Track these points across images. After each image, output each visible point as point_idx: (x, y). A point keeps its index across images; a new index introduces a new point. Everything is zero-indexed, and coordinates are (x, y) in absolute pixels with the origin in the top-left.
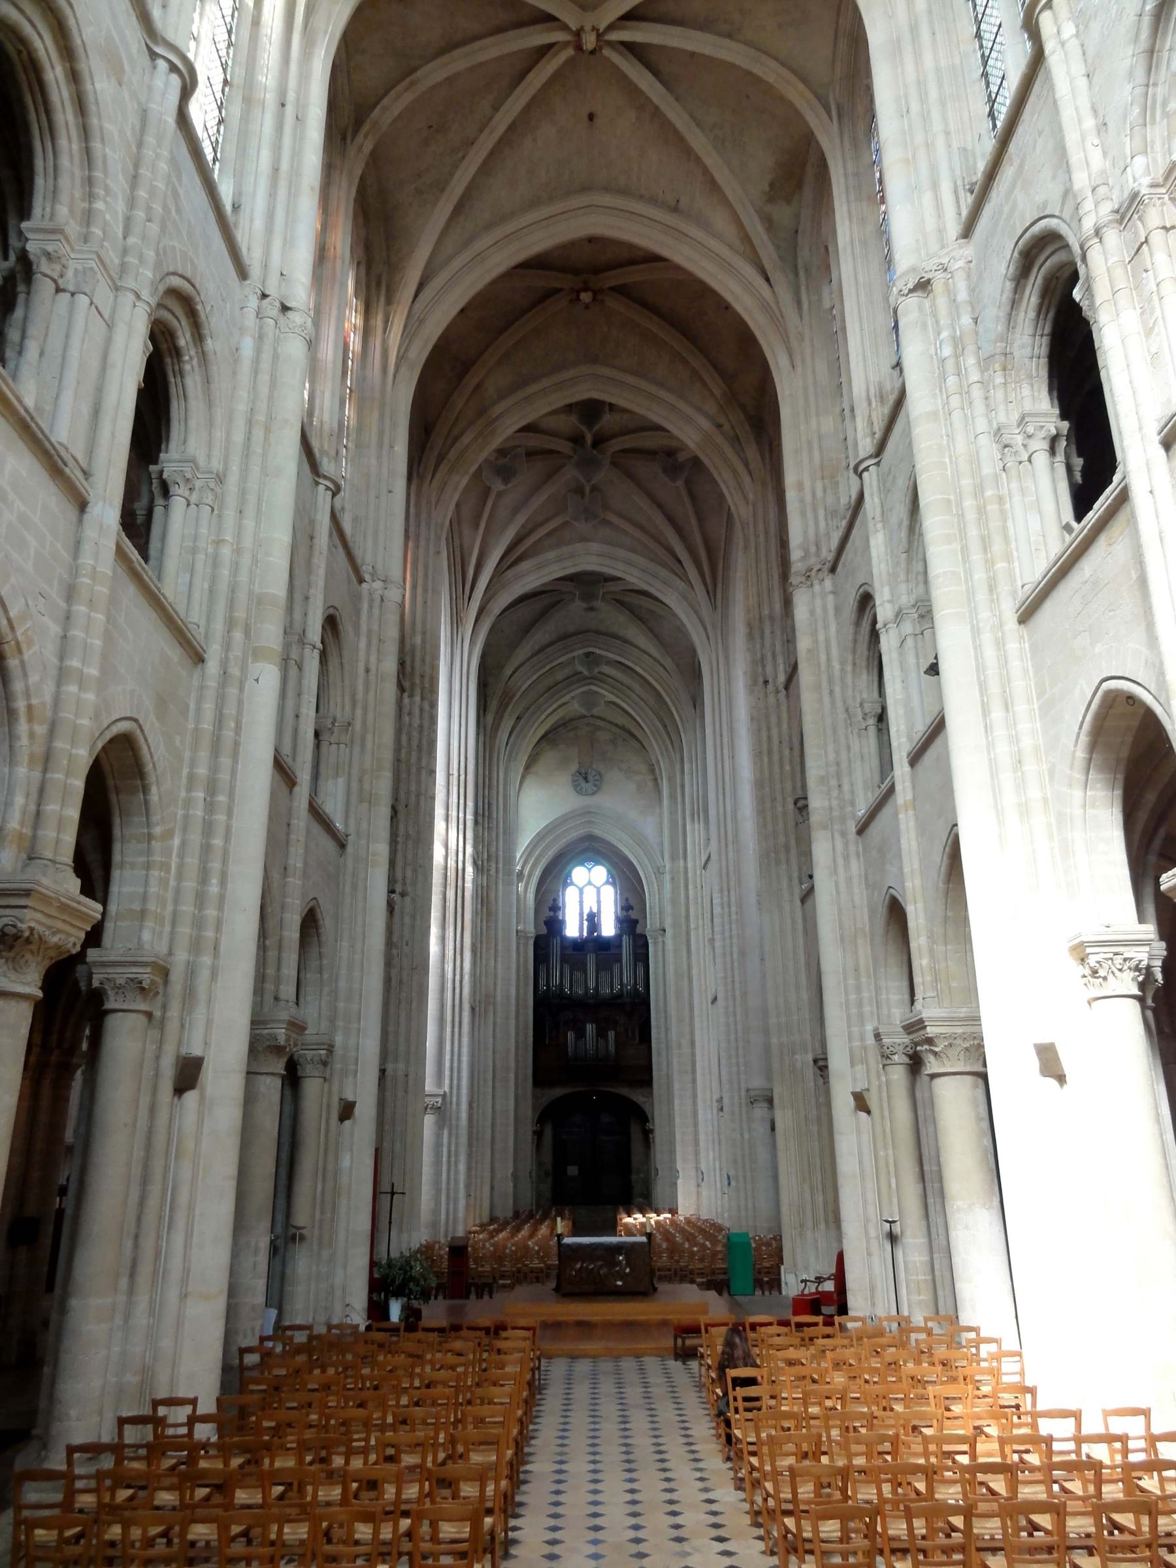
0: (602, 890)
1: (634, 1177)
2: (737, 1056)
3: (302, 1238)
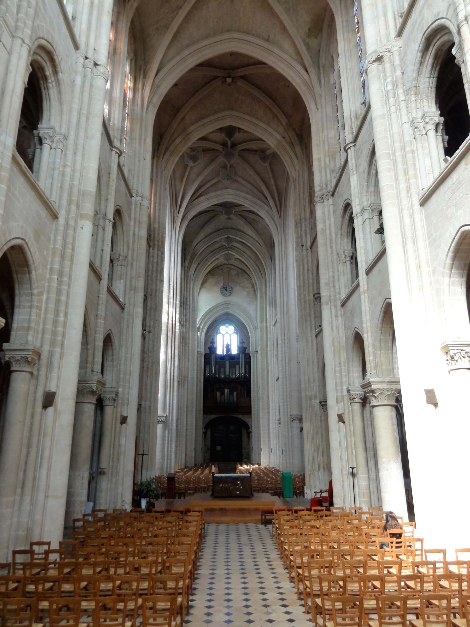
0: (232, 335)
1: (243, 451)
2: (287, 401)
3: (104, 473)
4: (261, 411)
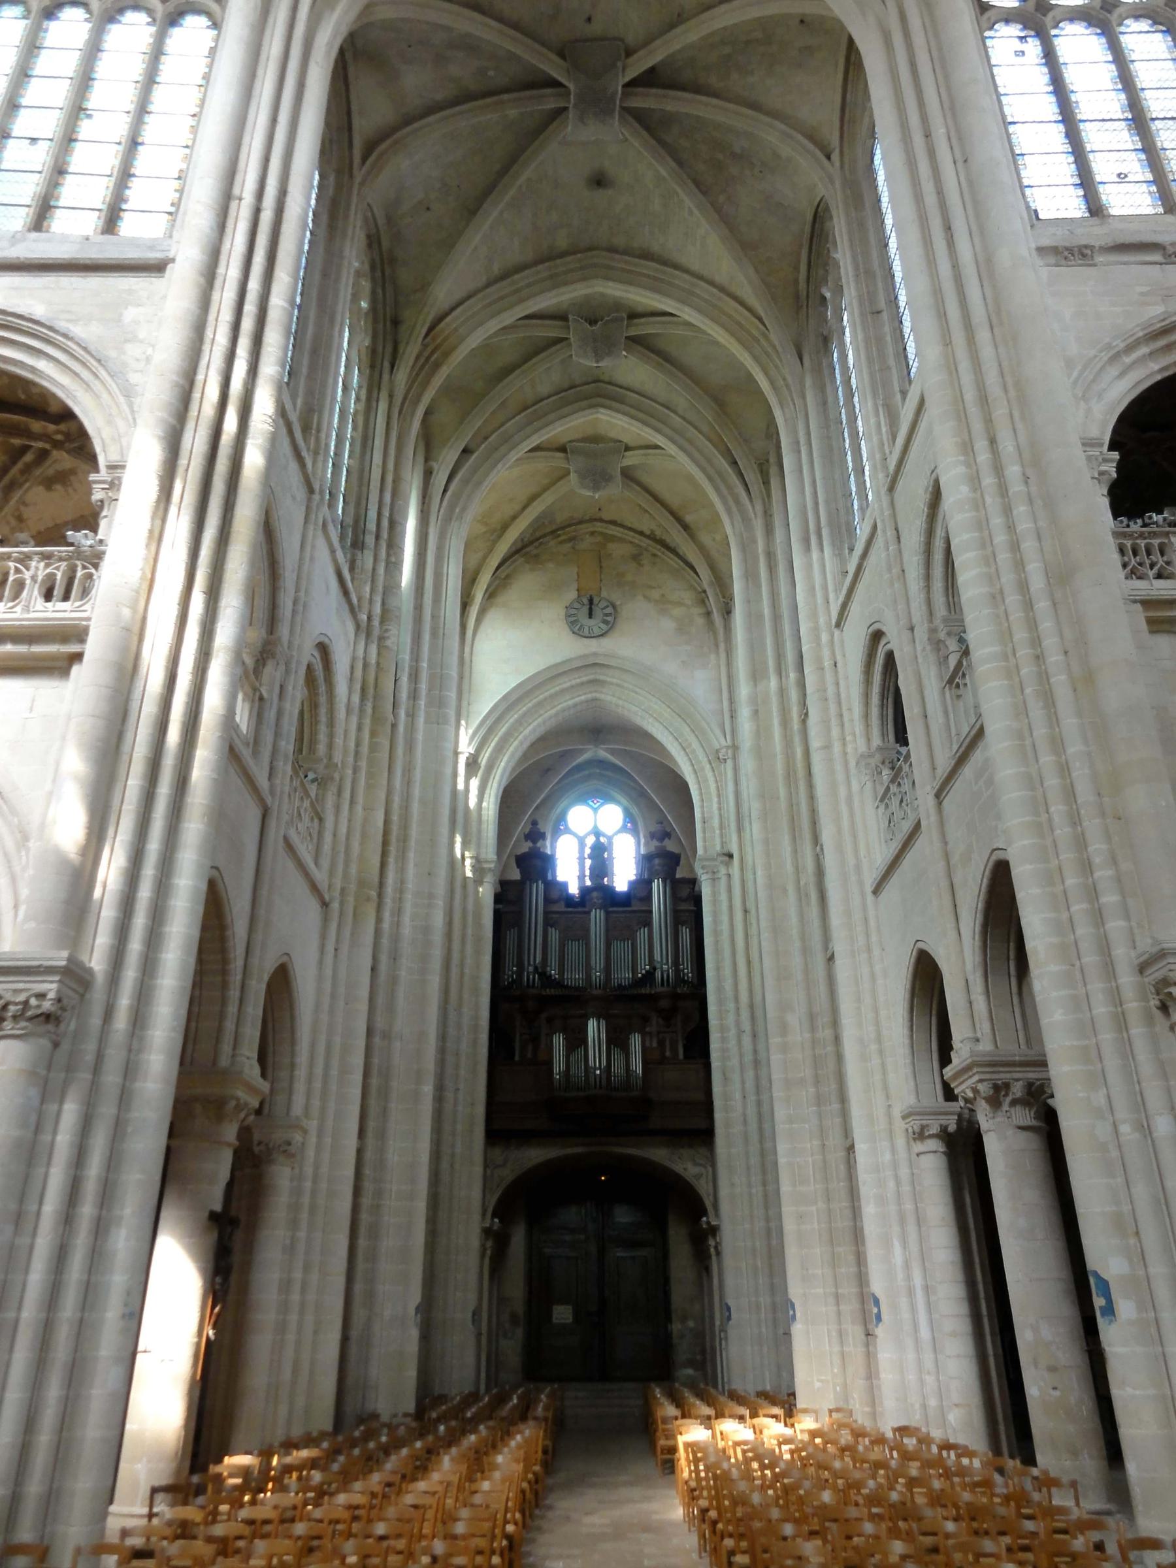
1: (676, 1327)
2: (1087, 867)
4: (778, 1093)
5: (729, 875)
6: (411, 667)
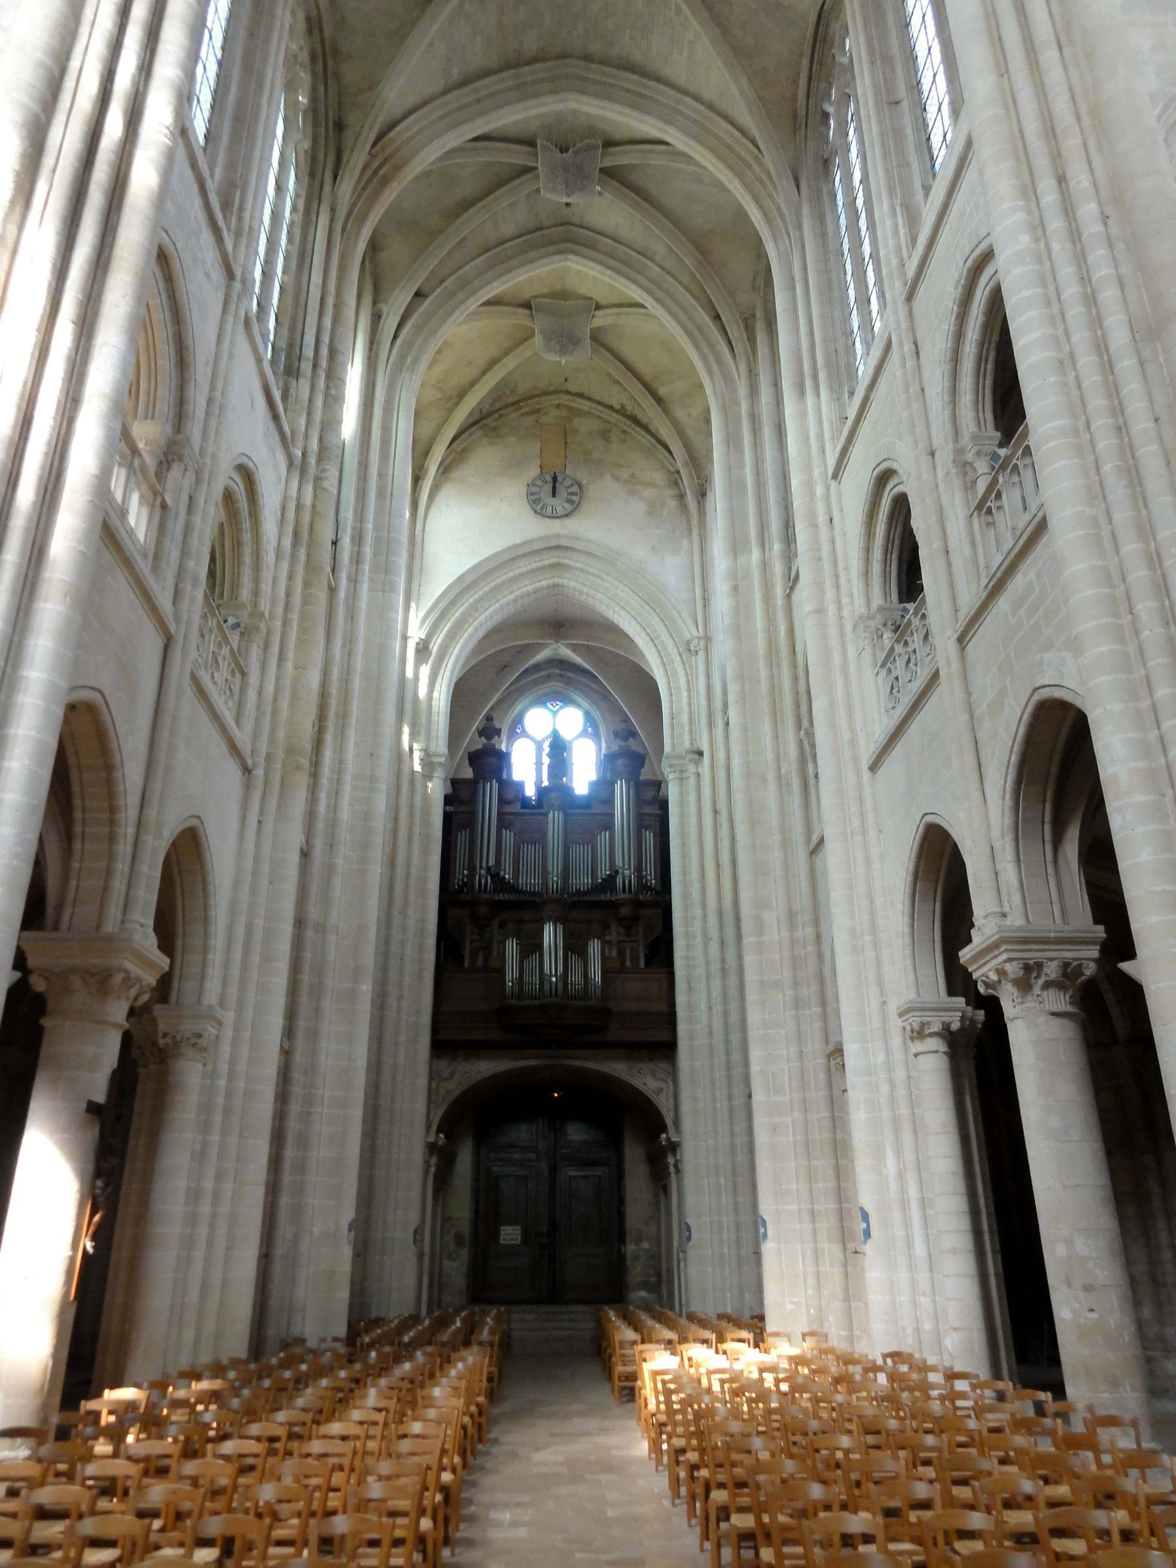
1: (630, 1248)
4: (752, 996)
5: (699, 775)
6: (354, 529)
